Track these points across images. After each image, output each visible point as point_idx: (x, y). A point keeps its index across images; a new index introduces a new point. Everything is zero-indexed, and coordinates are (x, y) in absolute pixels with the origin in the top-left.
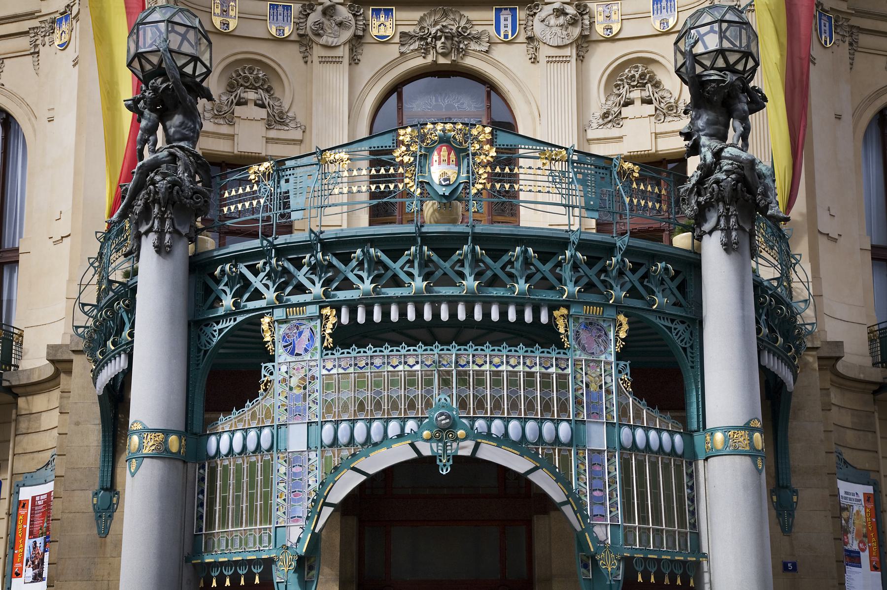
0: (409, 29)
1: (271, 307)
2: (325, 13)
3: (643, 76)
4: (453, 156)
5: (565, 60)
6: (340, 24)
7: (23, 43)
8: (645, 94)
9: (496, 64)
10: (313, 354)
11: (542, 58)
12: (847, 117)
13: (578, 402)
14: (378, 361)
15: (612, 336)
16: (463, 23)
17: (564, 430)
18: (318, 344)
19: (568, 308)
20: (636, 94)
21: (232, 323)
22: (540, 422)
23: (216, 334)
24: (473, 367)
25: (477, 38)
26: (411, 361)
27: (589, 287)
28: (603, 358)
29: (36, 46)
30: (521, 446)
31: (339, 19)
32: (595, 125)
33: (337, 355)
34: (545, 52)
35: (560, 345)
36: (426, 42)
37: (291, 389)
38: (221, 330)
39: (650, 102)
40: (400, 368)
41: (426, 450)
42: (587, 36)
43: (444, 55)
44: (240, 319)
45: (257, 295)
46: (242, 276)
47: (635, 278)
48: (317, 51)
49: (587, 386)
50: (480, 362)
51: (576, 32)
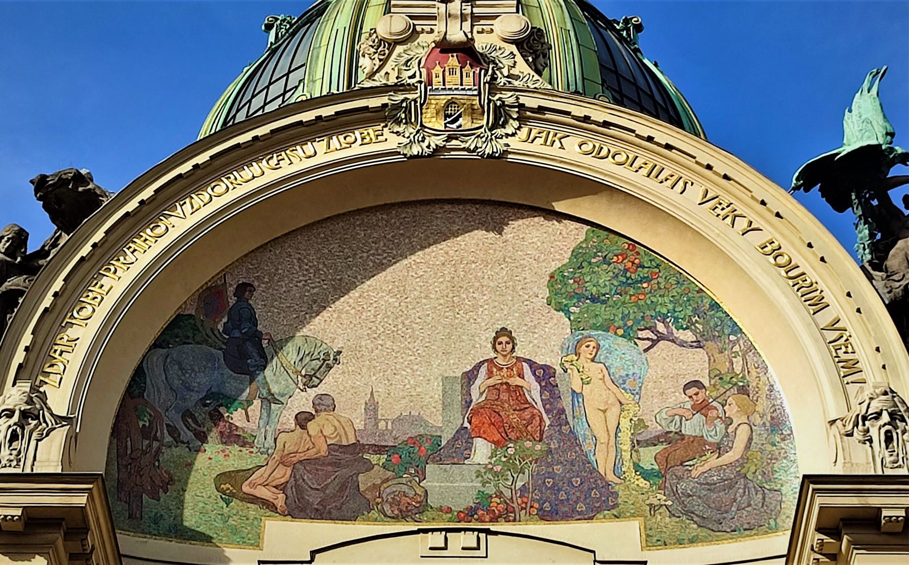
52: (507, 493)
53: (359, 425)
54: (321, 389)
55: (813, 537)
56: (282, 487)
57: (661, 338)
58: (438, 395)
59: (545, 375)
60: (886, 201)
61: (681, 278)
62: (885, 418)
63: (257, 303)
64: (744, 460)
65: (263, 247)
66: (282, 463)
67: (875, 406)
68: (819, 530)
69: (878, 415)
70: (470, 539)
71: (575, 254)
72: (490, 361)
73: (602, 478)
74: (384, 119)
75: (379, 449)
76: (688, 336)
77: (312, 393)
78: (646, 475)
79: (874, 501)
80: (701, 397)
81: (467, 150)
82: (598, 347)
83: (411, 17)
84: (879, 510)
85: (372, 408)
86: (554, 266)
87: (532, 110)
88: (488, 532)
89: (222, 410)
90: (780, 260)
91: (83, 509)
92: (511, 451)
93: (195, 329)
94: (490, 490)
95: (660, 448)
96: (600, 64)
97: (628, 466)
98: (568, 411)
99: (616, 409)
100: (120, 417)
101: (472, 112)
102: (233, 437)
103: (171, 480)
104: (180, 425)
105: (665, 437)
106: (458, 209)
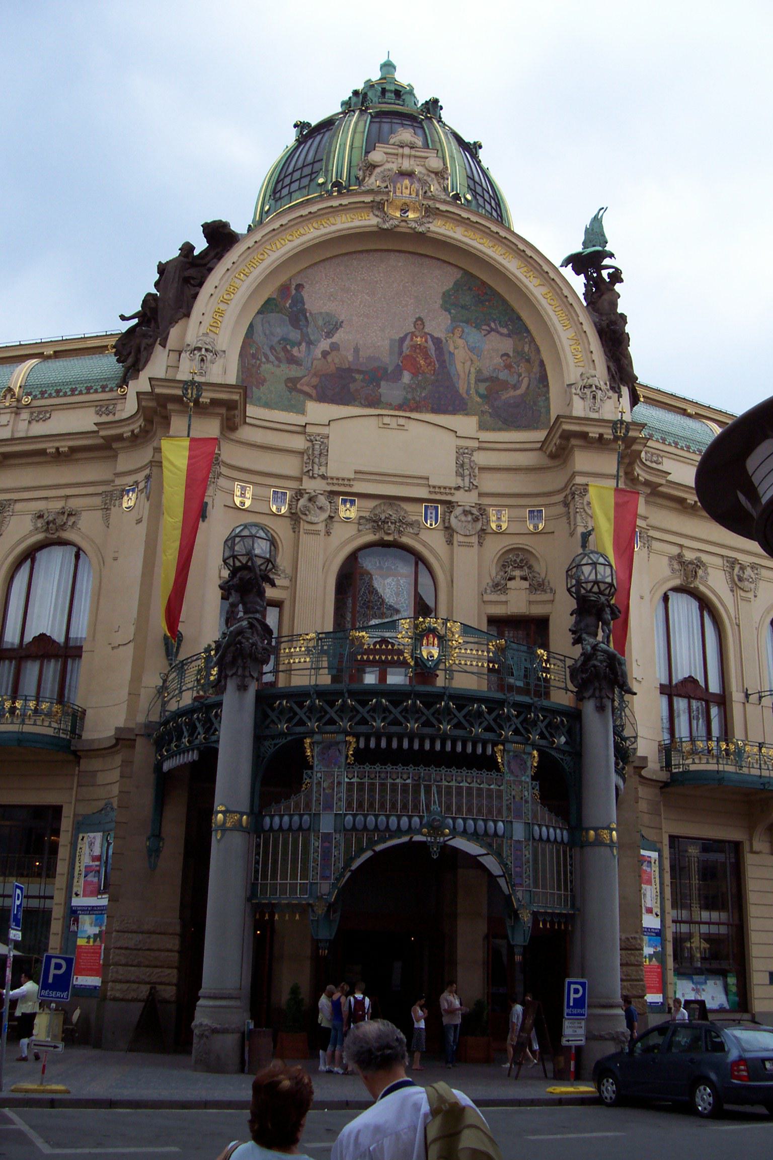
0: (366, 514)
1: (311, 733)
2: (310, 500)
3: (522, 561)
4: (436, 642)
5: (469, 545)
6: (321, 508)
7: (98, 501)
8: (523, 573)
9: (425, 544)
10: (339, 768)
11: (455, 543)
12: (647, 597)
13: (509, 809)
14: (383, 775)
15: (529, 764)
16: (402, 514)
17: (500, 824)
18: (343, 760)
19: (503, 745)
20: (517, 573)
21: (284, 741)
22: (485, 821)
23: (272, 747)
24: (445, 783)
25: (411, 525)
26: (405, 776)
27: (516, 732)
28: (523, 778)
29: (106, 504)
30: (475, 836)
31: (320, 505)
32: (488, 591)
33: (356, 769)
34: (457, 538)
35: (498, 770)
36: (377, 523)
37: (324, 789)
38: (275, 745)
39: (524, 578)
40: (398, 781)
41: (418, 838)
42: (484, 530)
43: (389, 534)
44: (289, 738)
45: (302, 723)
46: (291, 708)
47: (542, 725)
48: (304, 526)
49: (514, 797)
50: (449, 779)
51: (479, 526)
52: (418, 399)
53: (350, 358)
54: (334, 339)
55: (556, 440)
56: (315, 387)
57: (492, 330)
58: (387, 348)
59: (437, 342)
60: (600, 275)
61: (504, 301)
62: (594, 388)
63: (305, 294)
64: (526, 394)
65: (310, 267)
66: (315, 375)
67: (590, 381)
68: (561, 437)
69: (591, 386)
70: (402, 421)
71: (455, 284)
72: (413, 333)
73: (460, 395)
74: (372, 207)
75: (359, 372)
76: (505, 331)
77: (329, 341)
78: (481, 396)
79: (586, 429)
80: (508, 362)
81: (411, 228)
82: (463, 331)
83: (386, 153)
84: (588, 433)
85: (356, 350)
86: (445, 288)
87: (442, 211)
88: (409, 418)
89: (288, 347)
90: (552, 302)
91: (237, 401)
92: (420, 378)
93: (276, 305)
94: (409, 396)
95: (487, 384)
96: (468, 176)
97: (472, 391)
98: (447, 361)
99: (469, 363)
100: (242, 348)
101: (415, 210)
102: (292, 360)
103: (265, 380)
104: (269, 353)
105: (491, 379)
106: (402, 255)
